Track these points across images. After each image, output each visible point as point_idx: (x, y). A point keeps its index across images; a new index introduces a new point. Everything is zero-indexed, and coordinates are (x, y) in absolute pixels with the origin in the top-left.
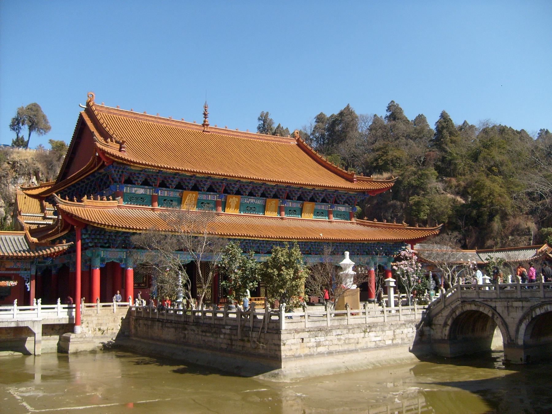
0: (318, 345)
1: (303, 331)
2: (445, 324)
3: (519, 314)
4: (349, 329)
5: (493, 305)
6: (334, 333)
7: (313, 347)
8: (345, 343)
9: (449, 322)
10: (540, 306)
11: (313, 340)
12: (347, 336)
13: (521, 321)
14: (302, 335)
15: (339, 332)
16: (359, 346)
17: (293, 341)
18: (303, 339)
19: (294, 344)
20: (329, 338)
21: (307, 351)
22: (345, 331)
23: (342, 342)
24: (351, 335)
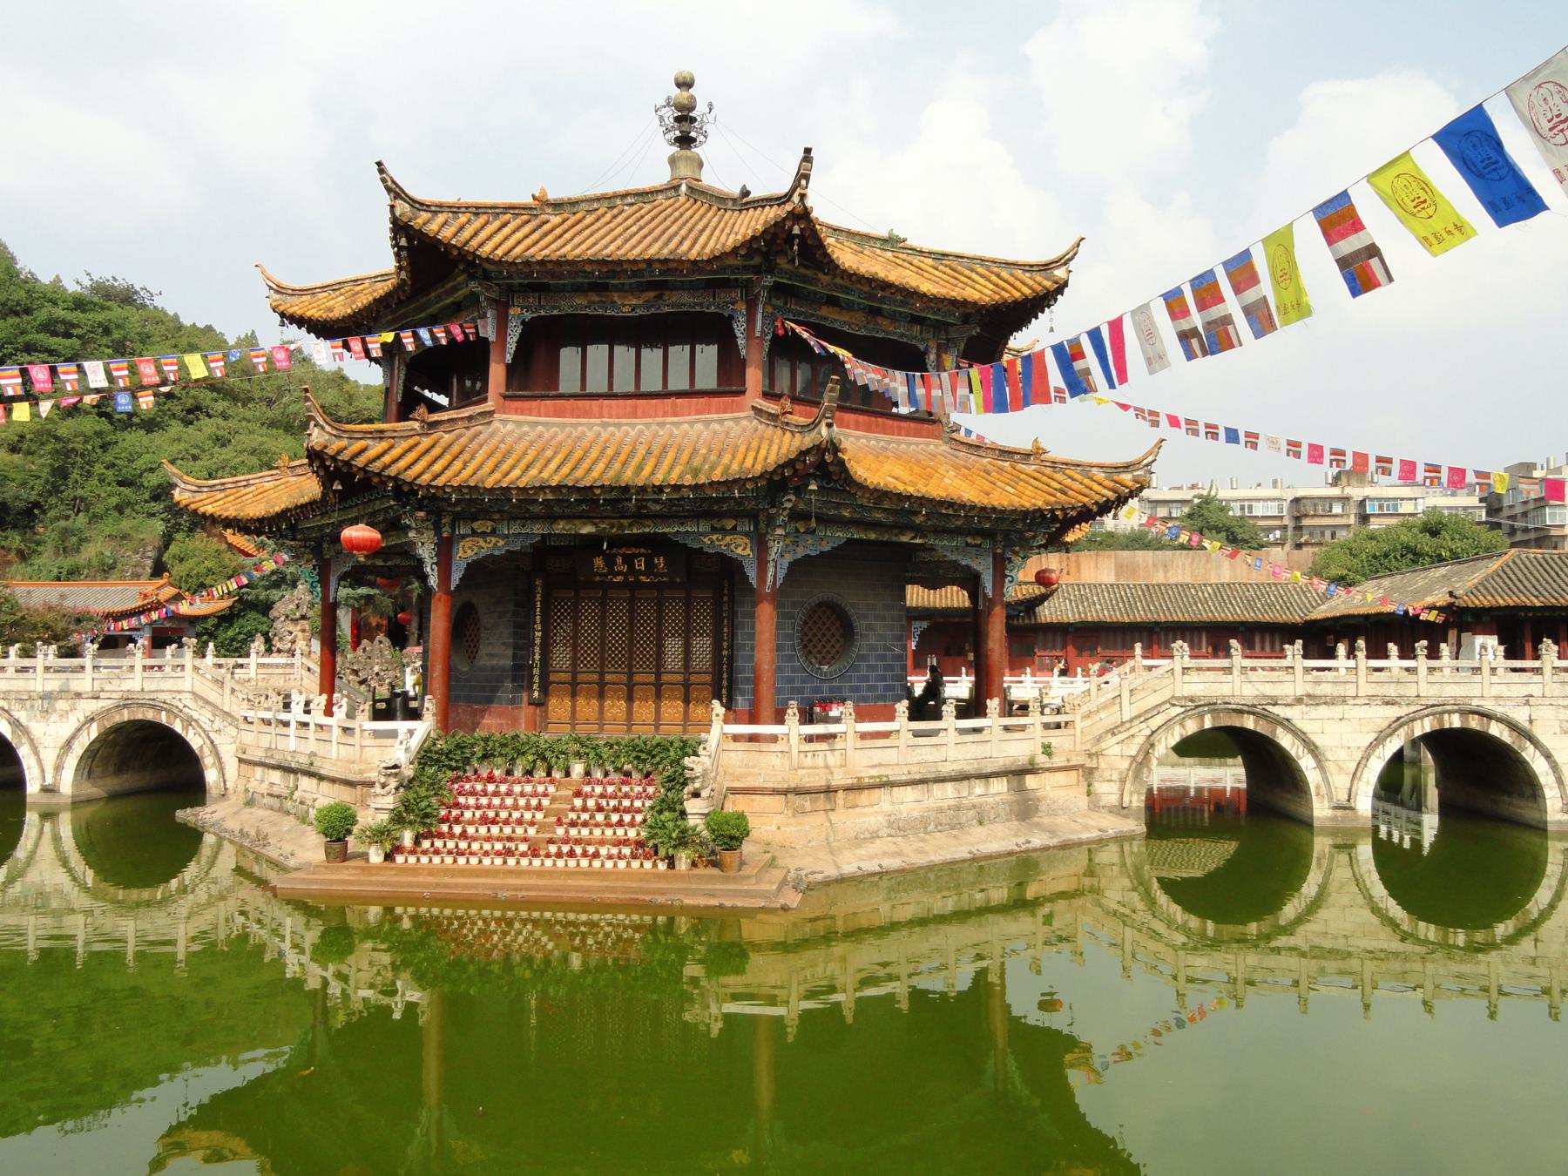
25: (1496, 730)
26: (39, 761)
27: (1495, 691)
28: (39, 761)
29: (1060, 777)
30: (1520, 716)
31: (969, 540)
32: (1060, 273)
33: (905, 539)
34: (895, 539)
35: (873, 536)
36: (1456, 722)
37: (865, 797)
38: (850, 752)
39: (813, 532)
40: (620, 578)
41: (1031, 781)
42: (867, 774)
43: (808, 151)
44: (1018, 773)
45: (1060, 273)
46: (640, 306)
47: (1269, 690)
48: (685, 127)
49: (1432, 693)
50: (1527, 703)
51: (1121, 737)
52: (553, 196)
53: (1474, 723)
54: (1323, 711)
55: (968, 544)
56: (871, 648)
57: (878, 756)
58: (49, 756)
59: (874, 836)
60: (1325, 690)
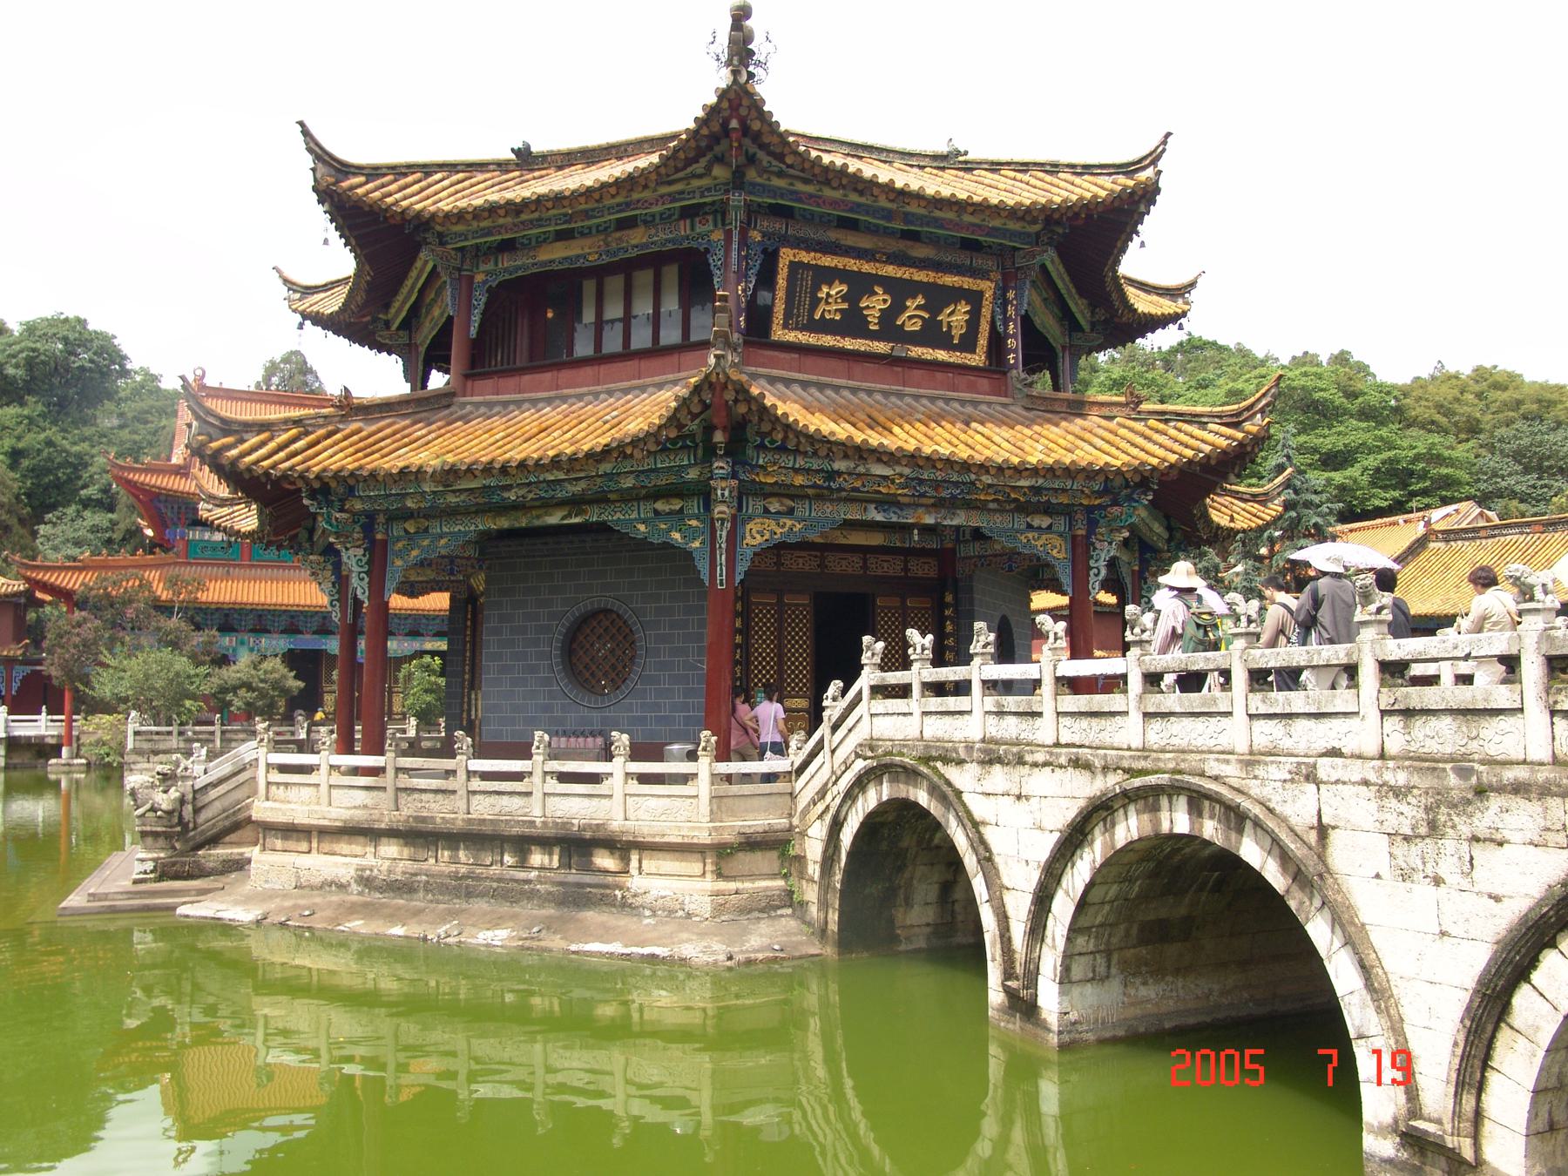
25: (1251, 852)
27: (1261, 742)
30: (1299, 807)
31: (659, 506)
33: (554, 519)
34: (537, 523)
35: (504, 523)
36: (1178, 820)
39: (426, 530)
43: (301, 124)
44: (577, 845)
47: (936, 729)
49: (1158, 734)
50: (1311, 777)
51: (820, 807)
53: (1210, 829)
54: (999, 777)
55: (656, 512)
60: (1010, 728)
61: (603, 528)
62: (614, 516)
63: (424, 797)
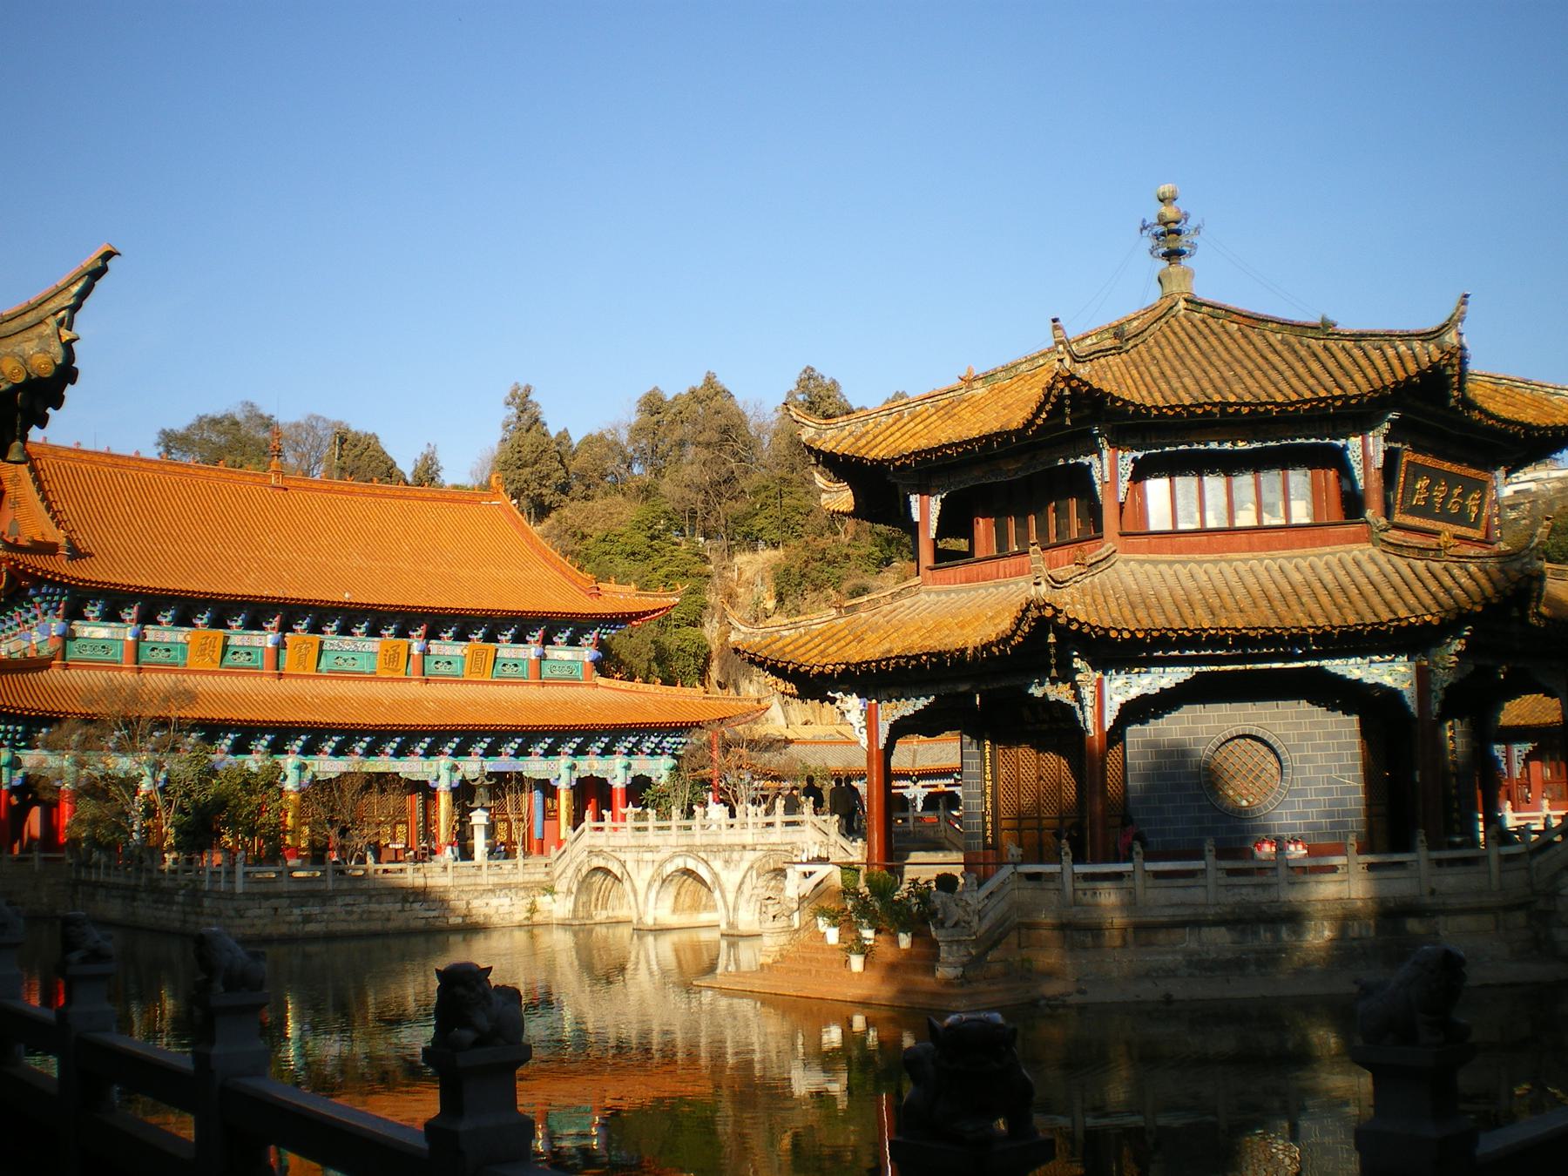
0: (307, 919)
1: (278, 895)
2: (569, 891)
3: (648, 872)
4: (371, 897)
5: (622, 856)
6: (340, 901)
7: (296, 923)
8: (361, 919)
9: (574, 890)
10: (672, 858)
11: (297, 911)
12: (365, 907)
13: (650, 885)
14: (274, 902)
15: (349, 900)
16: (391, 925)
17: (258, 912)
18: (276, 909)
19: (260, 917)
20: (329, 909)
21: (284, 929)
22: (363, 899)
23: (355, 917)
24: (374, 907)
26: (725, 902)
28: (725, 902)
29: (1467, 922)
32: (1450, 338)
37: (1161, 936)
38: (1139, 891)
40: (1045, 727)
41: (1413, 925)
42: (1165, 915)
45: (1450, 338)
46: (1020, 469)
48: (1171, 242)
52: (978, 371)
56: (1307, 782)
57: (1178, 895)
58: (730, 898)
59: (1171, 973)
61: (1320, 669)
62: (1335, 666)
63: (1244, 891)
